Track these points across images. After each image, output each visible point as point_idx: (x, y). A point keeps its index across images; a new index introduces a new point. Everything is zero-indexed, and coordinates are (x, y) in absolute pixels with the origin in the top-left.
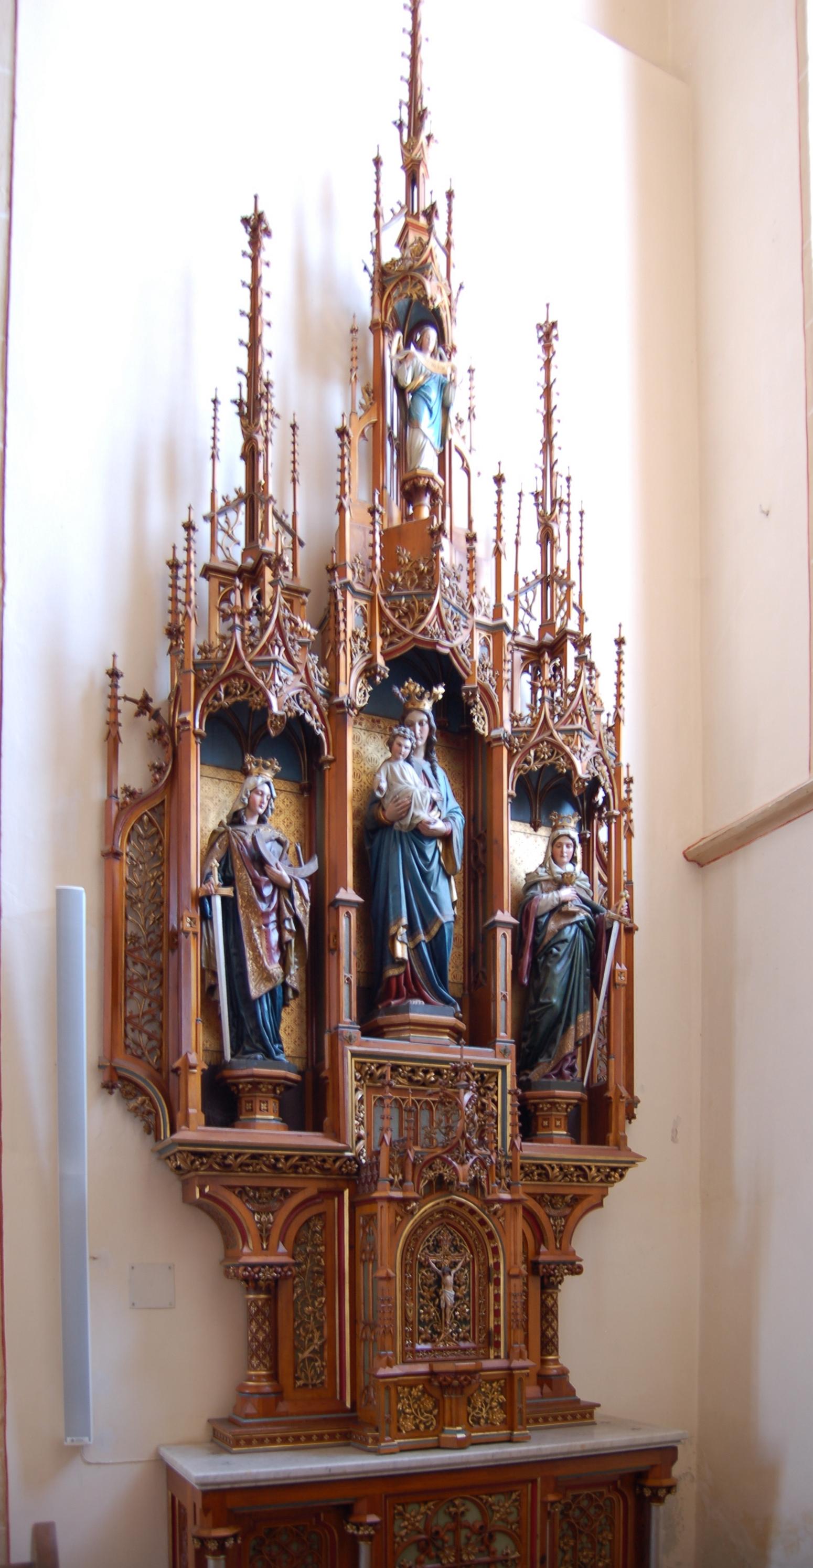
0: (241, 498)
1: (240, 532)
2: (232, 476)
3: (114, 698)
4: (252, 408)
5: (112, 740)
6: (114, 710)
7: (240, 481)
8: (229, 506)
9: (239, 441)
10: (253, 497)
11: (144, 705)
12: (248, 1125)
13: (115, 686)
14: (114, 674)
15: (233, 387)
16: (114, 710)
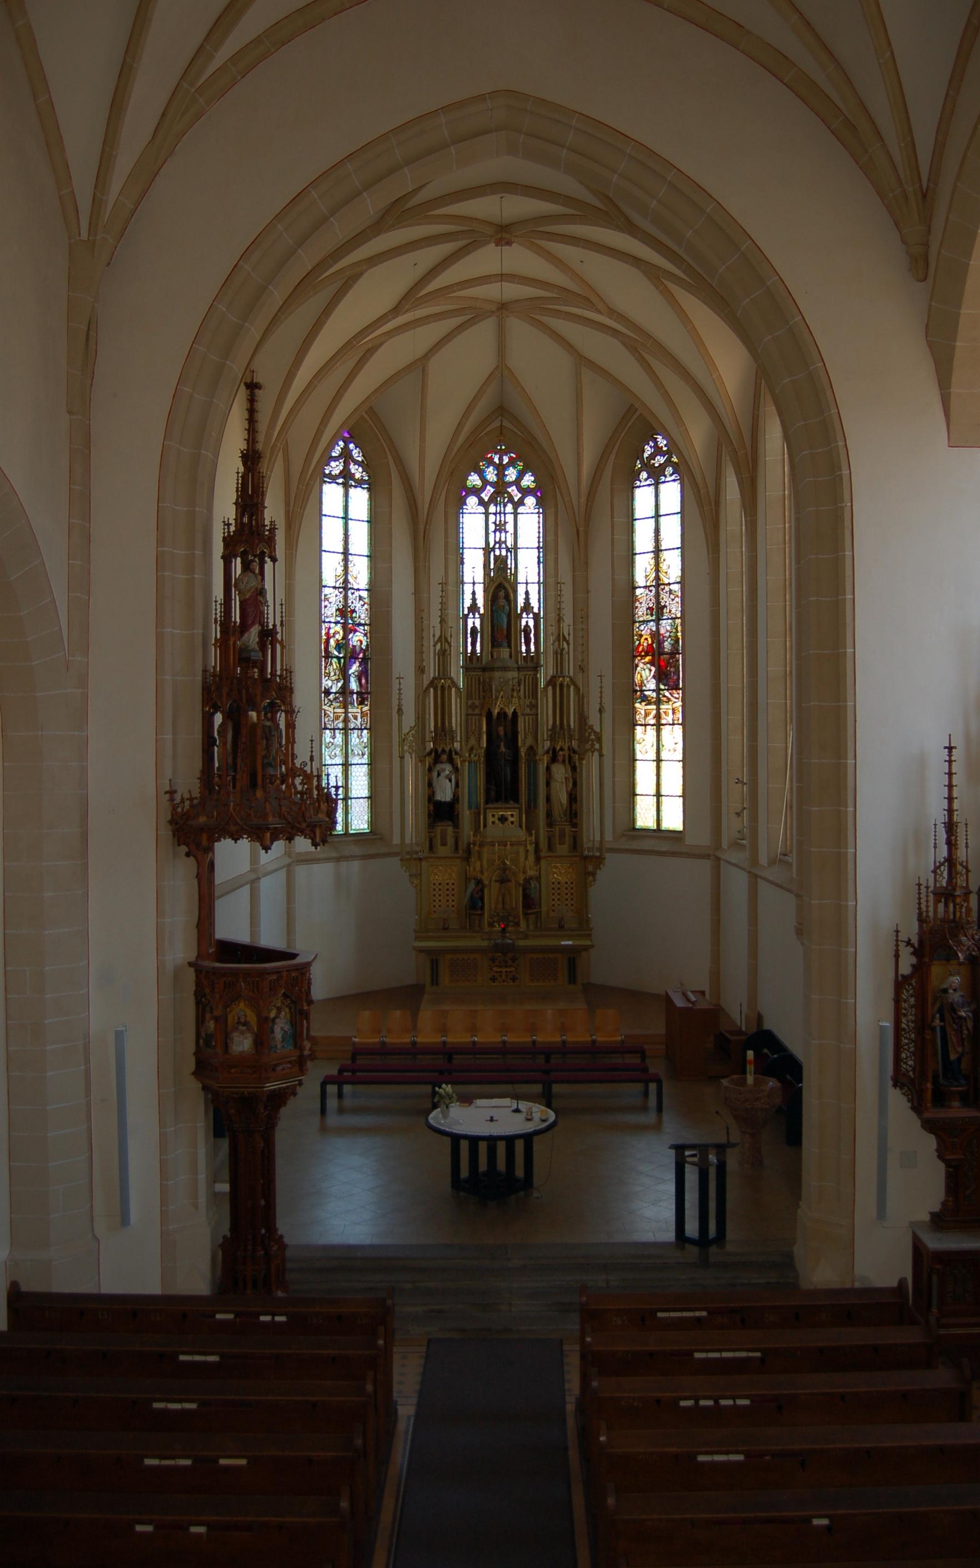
0: (946, 860)
1: (945, 874)
2: (943, 851)
3: (897, 941)
4: (950, 827)
5: (897, 956)
6: (897, 945)
7: (945, 854)
8: (942, 864)
9: (945, 836)
10: (950, 861)
11: (909, 943)
12: (950, 1107)
13: (897, 936)
14: (897, 932)
15: (942, 817)
16: (897, 945)
